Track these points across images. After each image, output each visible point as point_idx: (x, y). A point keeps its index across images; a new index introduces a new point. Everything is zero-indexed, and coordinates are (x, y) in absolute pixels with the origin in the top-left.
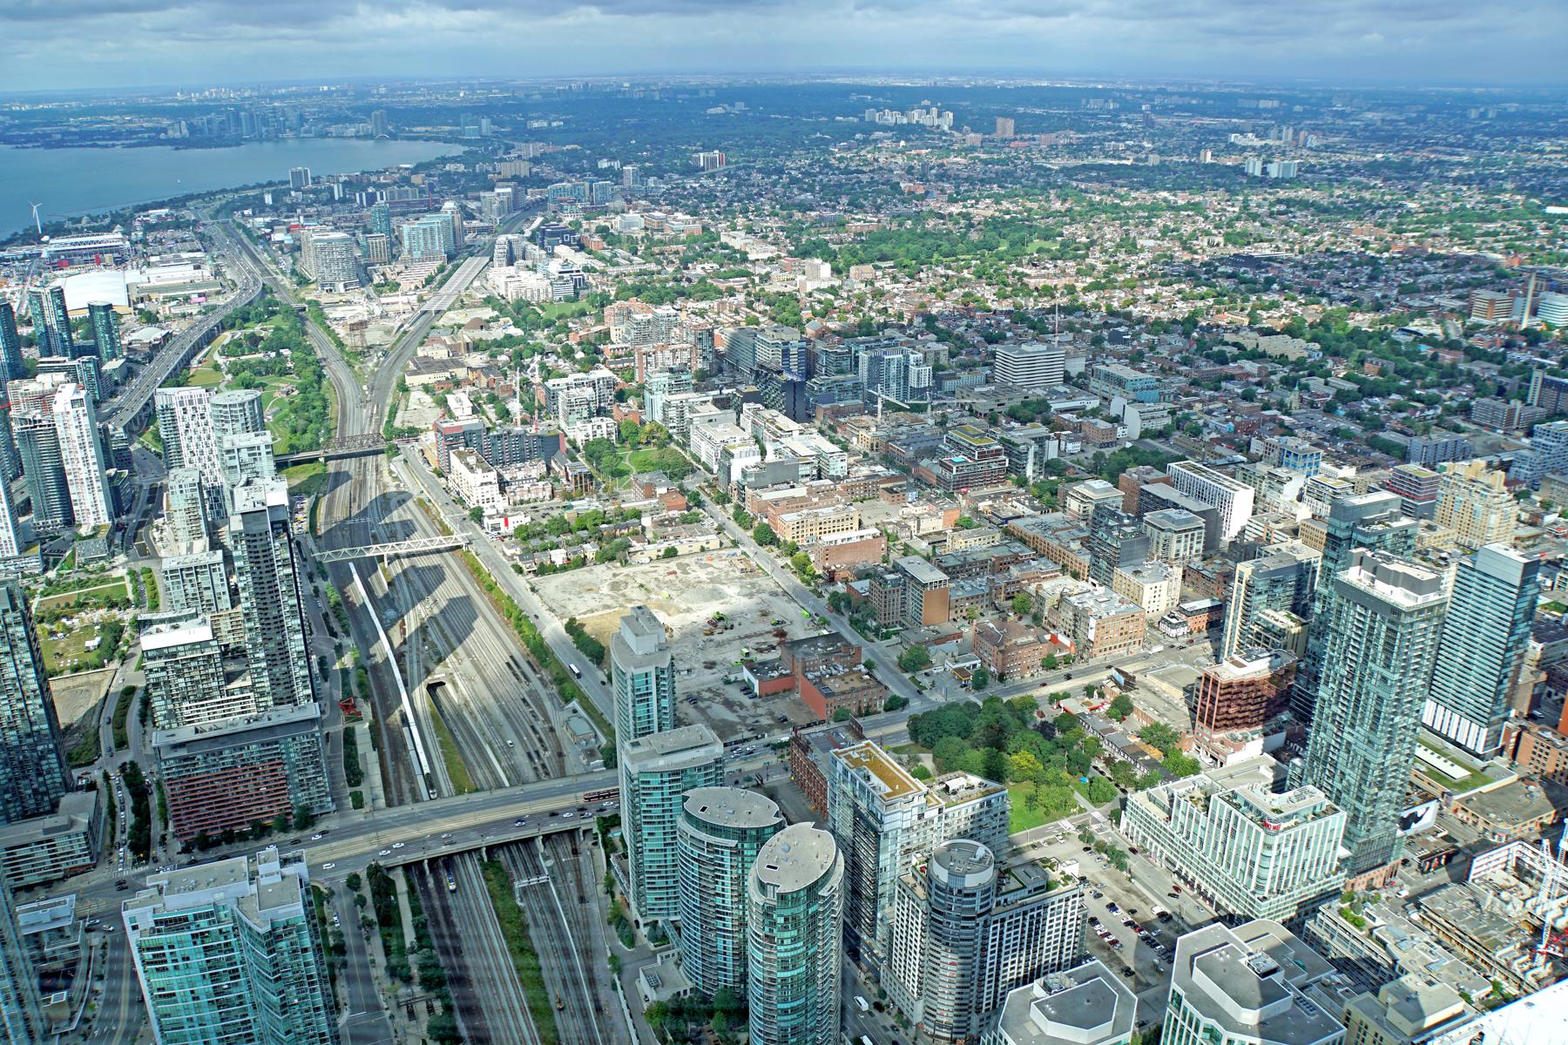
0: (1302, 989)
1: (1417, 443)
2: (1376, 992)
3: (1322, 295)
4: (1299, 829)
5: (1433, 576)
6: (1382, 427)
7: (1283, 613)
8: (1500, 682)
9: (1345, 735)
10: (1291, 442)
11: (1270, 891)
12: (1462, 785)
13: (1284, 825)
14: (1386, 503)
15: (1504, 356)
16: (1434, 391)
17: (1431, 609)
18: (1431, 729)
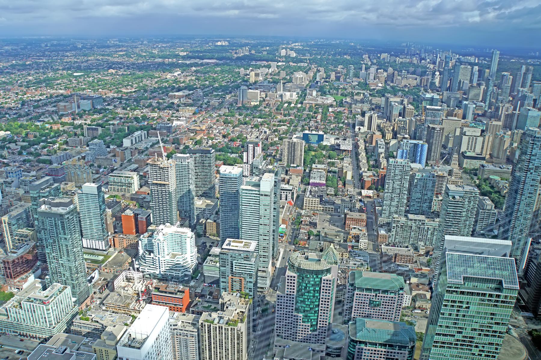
0: (77, 350)
1: (53, 157)
2: (100, 338)
3: (6, 114)
4: (57, 299)
5: (70, 200)
6: (40, 155)
7: (25, 229)
8: (102, 226)
9: (60, 262)
10: (9, 168)
11: (55, 324)
12: (103, 261)
13: (50, 300)
14: (48, 181)
15: (73, 122)
16: (54, 139)
17: (72, 211)
18: (87, 248)
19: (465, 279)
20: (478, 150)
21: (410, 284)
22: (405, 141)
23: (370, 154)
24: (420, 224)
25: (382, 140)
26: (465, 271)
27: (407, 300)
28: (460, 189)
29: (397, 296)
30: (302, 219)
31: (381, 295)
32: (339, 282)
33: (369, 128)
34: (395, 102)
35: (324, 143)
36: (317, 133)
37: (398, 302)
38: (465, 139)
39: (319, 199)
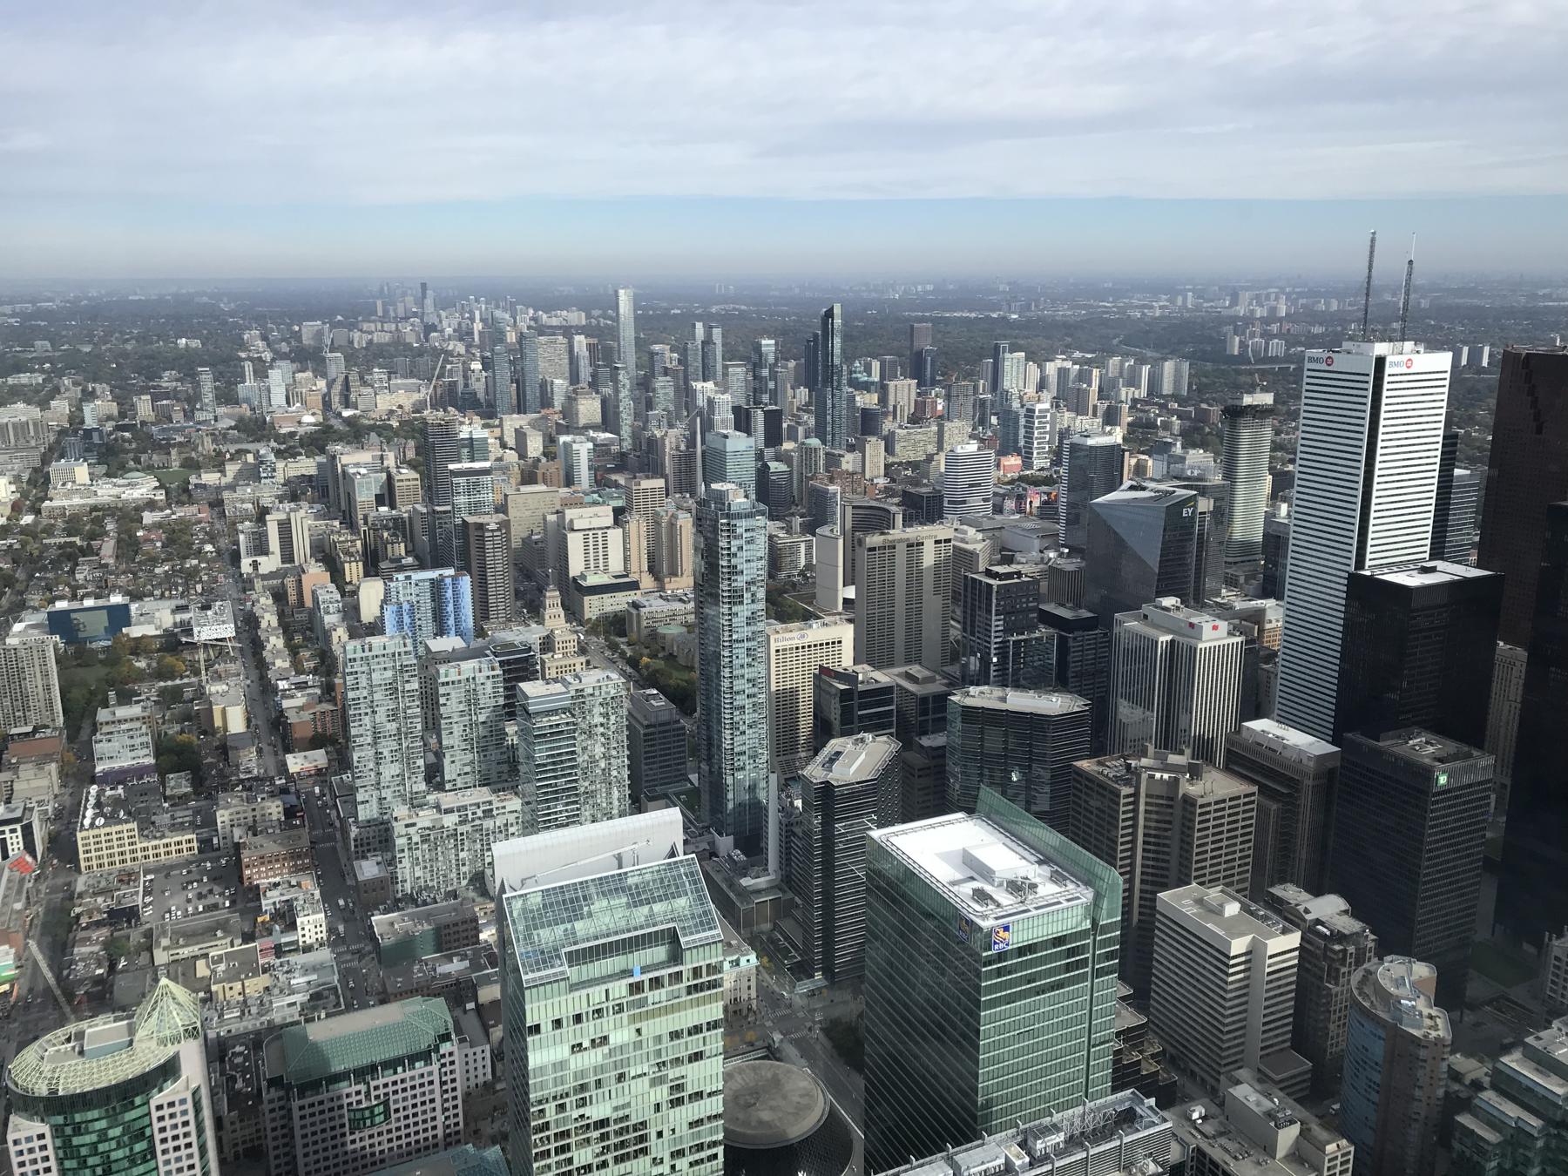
19: (570, 955)
20: (616, 565)
21: (479, 1008)
22: (401, 576)
23: (298, 639)
24: (480, 814)
25: (332, 587)
26: (571, 936)
27: (480, 1064)
28: (559, 688)
29: (435, 1067)
30: (78, 910)
31: (381, 1081)
32: (239, 1085)
33: (287, 556)
34: (357, 465)
35: (135, 631)
36: (101, 602)
37: (443, 1083)
38: (575, 543)
39: (134, 825)
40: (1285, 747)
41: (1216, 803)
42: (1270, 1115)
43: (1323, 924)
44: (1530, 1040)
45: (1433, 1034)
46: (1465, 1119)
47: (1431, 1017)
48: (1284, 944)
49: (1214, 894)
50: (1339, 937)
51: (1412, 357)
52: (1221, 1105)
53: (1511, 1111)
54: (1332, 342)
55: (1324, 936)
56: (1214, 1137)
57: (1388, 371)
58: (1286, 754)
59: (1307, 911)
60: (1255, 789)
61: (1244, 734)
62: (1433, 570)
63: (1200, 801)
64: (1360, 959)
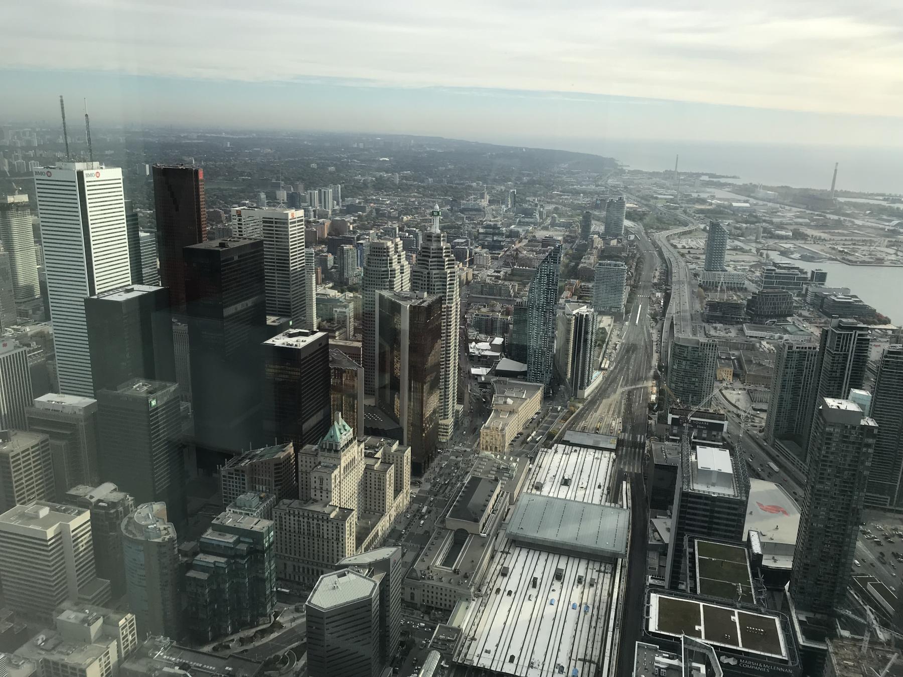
40: (64, 407)
41: (23, 452)
42: (84, 621)
43: (102, 501)
44: (214, 522)
45: (168, 537)
46: (191, 574)
47: (165, 529)
48: (80, 521)
49: (30, 508)
50: (113, 505)
51: (99, 171)
52: (55, 628)
53: (211, 559)
54: (47, 163)
55: (103, 507)
56: (53, 649)
57: (86, 179)
58: (65, 411)
59: (92, 497)
60: (47, 436)
61: (37, 406)
62: (132, 290)
63: (11, 455)
64: (127, 511)
